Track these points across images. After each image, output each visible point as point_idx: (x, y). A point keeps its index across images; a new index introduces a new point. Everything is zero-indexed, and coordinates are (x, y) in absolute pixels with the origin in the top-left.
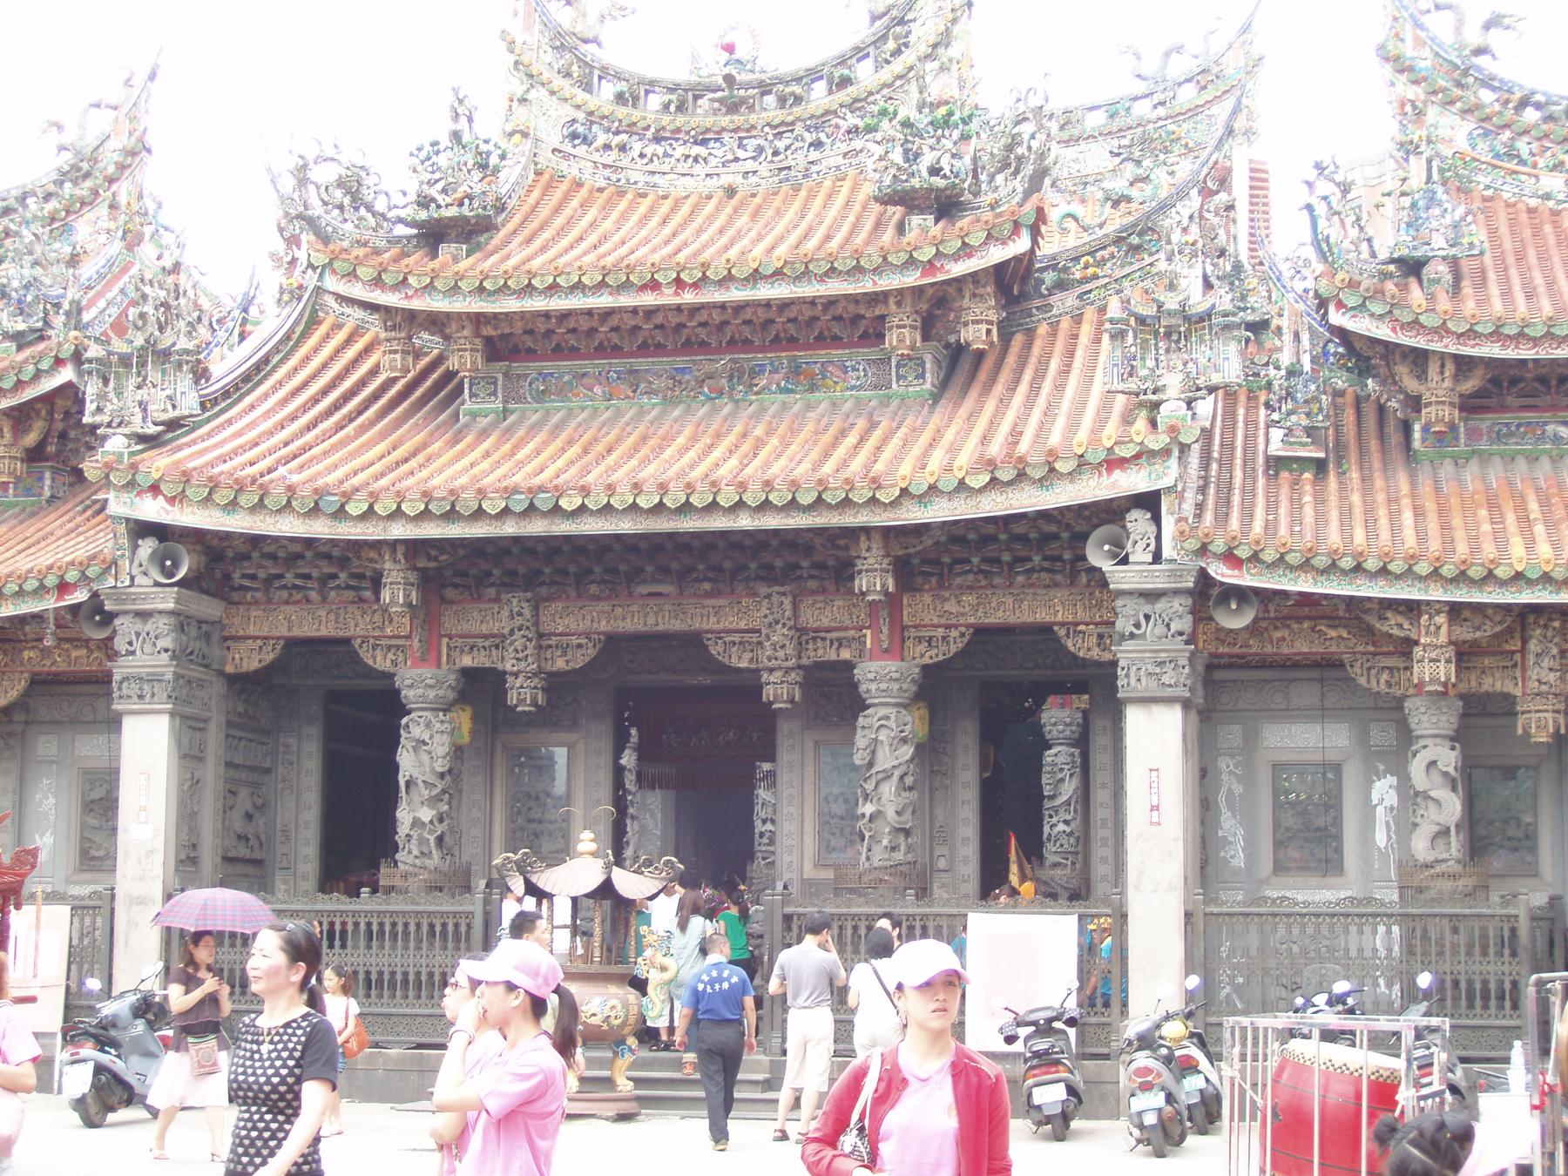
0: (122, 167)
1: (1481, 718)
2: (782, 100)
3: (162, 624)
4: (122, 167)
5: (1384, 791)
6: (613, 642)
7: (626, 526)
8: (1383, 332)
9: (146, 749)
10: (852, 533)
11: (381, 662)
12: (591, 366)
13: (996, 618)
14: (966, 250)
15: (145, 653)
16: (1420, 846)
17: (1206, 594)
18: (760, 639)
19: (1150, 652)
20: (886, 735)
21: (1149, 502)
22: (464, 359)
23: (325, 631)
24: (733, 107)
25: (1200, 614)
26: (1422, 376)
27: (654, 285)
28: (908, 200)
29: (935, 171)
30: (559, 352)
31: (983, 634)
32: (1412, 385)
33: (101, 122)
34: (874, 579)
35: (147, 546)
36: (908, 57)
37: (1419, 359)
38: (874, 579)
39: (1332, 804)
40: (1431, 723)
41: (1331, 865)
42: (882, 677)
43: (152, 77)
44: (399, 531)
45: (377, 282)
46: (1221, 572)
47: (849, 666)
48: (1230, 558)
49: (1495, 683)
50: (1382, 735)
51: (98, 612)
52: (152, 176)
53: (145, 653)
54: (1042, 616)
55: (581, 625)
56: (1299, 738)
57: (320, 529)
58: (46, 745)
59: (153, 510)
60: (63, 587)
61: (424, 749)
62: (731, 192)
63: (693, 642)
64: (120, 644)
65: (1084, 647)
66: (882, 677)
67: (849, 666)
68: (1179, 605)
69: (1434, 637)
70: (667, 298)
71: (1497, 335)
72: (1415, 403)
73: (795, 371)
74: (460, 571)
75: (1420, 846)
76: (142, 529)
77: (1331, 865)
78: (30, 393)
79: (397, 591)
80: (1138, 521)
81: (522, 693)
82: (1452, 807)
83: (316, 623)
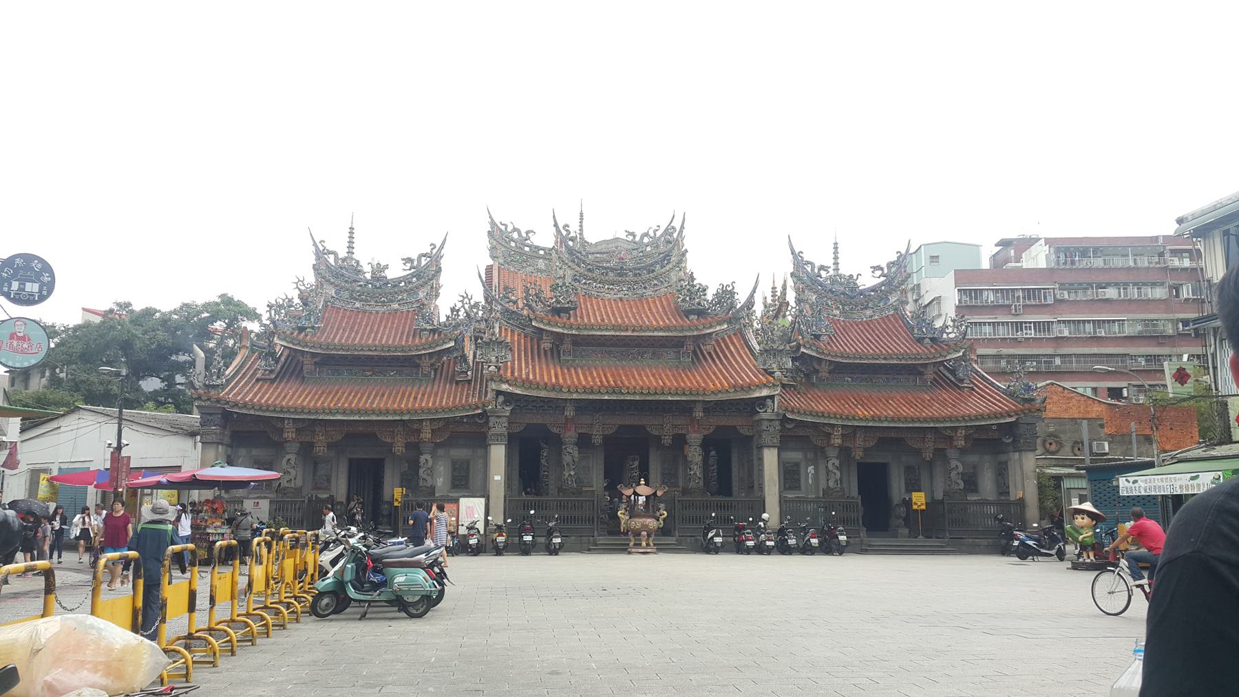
0: (434, 276)
1: (845, 453)
2: (635, 275)
3: (505, 419)
4: (434, 276)
5: (811, 469)
6: (621, 426)
7: (638, 398)
8: (814, 354)
9: (498, 453)
10: (695, 402)
11: (555, 430)
12: (599, 349)
13: (723, 423)
14: (711, 327)
15: (499, 427)
16: (831, 484)
17: (784, 420)
18: (665, 429)
19: (771, 432)
20: (694, 454)
21: (772, 397)
22: (567, 346)
23: (540, 422)
24: (620, 275)
25: (782, 424)
26: (820, 364)
27: (627, 330)
28: (688, 313)
29: (699, 304)
30: (588, 344)
31: (718, 428)
32: (817, 367)
33: (424, 261)
34: (699, 414)
35: (501, 399)
36: (670, 266)
37: (819, 360)
38: (699, 414)
39: (797, 472)
40: (832, 453)
41: (798, 488)
42: (695, 438)
43: (442, 247)
44: (575, 396)
45: (549, 324)
46: (789, 416)
47: (684, 435)
48: (793, 412)
49: (848, 444)
50: (810, 455)
51: (484, 414)
52: (443, 279)
53: (499, 427)
54: (734, 423)
55: (614, 422)
56: (794, 456)
57: (552, 395)
58: (441, 452)
59: (504, 387)
60: (477, 408)
61: (571, 453)
62: (621, 299)
63: (643, 427)
64: (491, 424)
65: (745, 431)
66: (695, 438)
67: (684, 435)
68: (777, 423)
69: (838, 433)
70: (629, 333)
71: (842, 357)
72: (817, 371)
73: (654, 354)
74: (588, 407)
75: (831, 484)
76: (499, 393)
77: (798, 488)
78: (438, 349)
79: (570, 413)
80: (769, 402)
81: (597, 440)
82: (838, 473)
83: (538, 419)
